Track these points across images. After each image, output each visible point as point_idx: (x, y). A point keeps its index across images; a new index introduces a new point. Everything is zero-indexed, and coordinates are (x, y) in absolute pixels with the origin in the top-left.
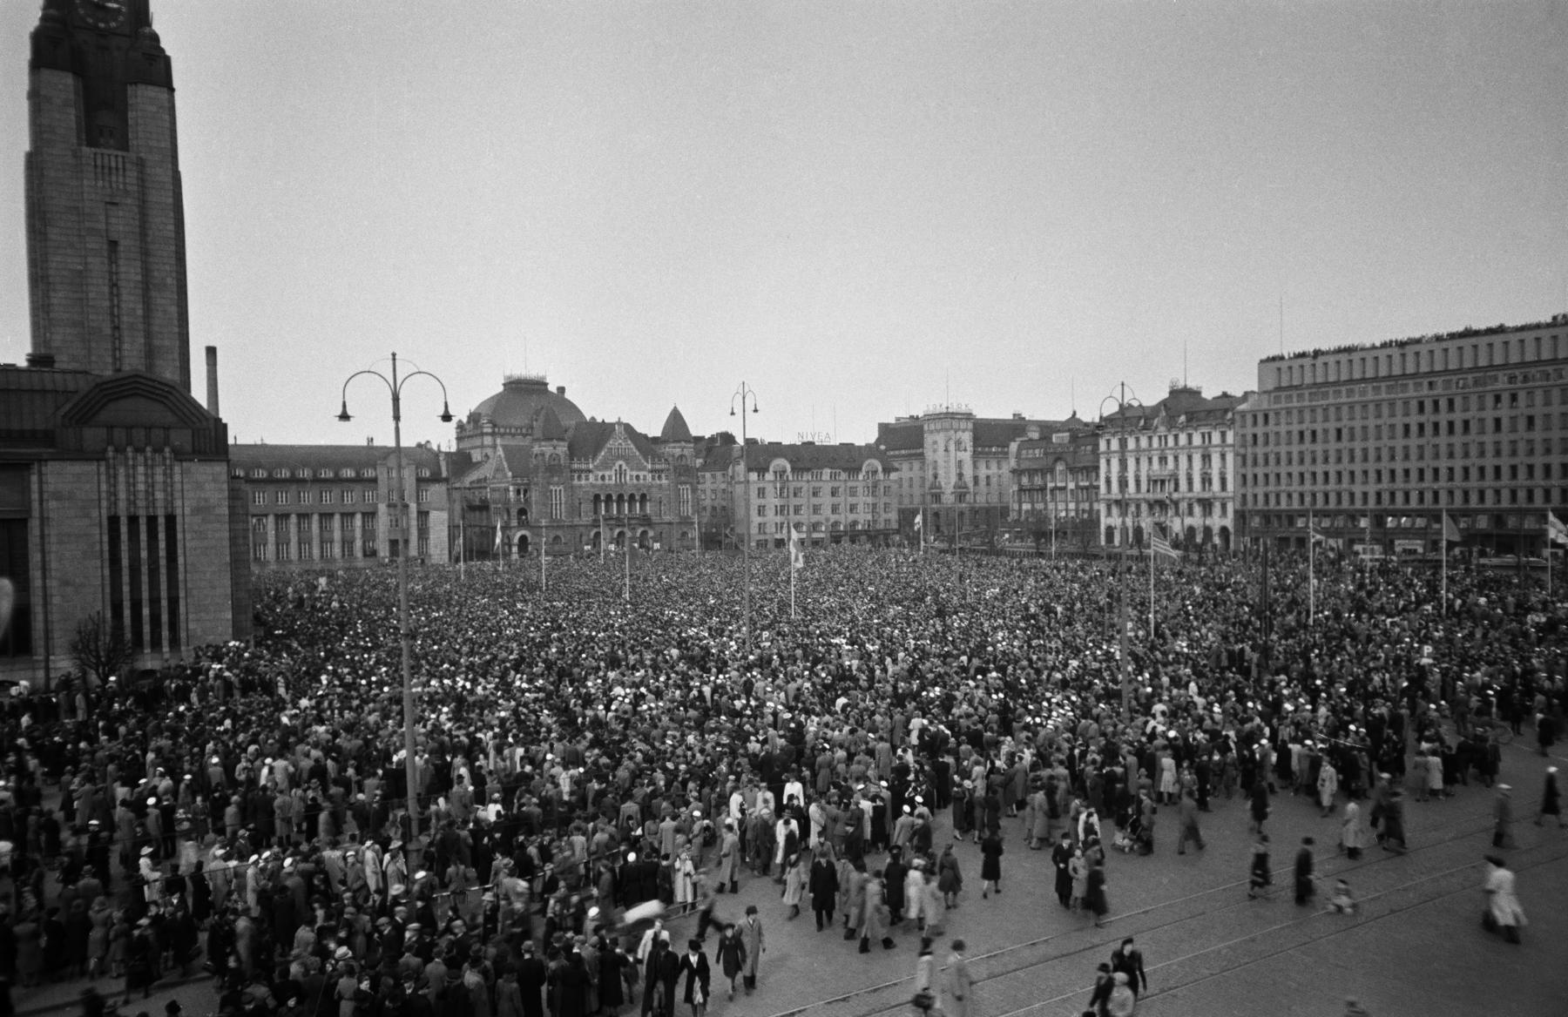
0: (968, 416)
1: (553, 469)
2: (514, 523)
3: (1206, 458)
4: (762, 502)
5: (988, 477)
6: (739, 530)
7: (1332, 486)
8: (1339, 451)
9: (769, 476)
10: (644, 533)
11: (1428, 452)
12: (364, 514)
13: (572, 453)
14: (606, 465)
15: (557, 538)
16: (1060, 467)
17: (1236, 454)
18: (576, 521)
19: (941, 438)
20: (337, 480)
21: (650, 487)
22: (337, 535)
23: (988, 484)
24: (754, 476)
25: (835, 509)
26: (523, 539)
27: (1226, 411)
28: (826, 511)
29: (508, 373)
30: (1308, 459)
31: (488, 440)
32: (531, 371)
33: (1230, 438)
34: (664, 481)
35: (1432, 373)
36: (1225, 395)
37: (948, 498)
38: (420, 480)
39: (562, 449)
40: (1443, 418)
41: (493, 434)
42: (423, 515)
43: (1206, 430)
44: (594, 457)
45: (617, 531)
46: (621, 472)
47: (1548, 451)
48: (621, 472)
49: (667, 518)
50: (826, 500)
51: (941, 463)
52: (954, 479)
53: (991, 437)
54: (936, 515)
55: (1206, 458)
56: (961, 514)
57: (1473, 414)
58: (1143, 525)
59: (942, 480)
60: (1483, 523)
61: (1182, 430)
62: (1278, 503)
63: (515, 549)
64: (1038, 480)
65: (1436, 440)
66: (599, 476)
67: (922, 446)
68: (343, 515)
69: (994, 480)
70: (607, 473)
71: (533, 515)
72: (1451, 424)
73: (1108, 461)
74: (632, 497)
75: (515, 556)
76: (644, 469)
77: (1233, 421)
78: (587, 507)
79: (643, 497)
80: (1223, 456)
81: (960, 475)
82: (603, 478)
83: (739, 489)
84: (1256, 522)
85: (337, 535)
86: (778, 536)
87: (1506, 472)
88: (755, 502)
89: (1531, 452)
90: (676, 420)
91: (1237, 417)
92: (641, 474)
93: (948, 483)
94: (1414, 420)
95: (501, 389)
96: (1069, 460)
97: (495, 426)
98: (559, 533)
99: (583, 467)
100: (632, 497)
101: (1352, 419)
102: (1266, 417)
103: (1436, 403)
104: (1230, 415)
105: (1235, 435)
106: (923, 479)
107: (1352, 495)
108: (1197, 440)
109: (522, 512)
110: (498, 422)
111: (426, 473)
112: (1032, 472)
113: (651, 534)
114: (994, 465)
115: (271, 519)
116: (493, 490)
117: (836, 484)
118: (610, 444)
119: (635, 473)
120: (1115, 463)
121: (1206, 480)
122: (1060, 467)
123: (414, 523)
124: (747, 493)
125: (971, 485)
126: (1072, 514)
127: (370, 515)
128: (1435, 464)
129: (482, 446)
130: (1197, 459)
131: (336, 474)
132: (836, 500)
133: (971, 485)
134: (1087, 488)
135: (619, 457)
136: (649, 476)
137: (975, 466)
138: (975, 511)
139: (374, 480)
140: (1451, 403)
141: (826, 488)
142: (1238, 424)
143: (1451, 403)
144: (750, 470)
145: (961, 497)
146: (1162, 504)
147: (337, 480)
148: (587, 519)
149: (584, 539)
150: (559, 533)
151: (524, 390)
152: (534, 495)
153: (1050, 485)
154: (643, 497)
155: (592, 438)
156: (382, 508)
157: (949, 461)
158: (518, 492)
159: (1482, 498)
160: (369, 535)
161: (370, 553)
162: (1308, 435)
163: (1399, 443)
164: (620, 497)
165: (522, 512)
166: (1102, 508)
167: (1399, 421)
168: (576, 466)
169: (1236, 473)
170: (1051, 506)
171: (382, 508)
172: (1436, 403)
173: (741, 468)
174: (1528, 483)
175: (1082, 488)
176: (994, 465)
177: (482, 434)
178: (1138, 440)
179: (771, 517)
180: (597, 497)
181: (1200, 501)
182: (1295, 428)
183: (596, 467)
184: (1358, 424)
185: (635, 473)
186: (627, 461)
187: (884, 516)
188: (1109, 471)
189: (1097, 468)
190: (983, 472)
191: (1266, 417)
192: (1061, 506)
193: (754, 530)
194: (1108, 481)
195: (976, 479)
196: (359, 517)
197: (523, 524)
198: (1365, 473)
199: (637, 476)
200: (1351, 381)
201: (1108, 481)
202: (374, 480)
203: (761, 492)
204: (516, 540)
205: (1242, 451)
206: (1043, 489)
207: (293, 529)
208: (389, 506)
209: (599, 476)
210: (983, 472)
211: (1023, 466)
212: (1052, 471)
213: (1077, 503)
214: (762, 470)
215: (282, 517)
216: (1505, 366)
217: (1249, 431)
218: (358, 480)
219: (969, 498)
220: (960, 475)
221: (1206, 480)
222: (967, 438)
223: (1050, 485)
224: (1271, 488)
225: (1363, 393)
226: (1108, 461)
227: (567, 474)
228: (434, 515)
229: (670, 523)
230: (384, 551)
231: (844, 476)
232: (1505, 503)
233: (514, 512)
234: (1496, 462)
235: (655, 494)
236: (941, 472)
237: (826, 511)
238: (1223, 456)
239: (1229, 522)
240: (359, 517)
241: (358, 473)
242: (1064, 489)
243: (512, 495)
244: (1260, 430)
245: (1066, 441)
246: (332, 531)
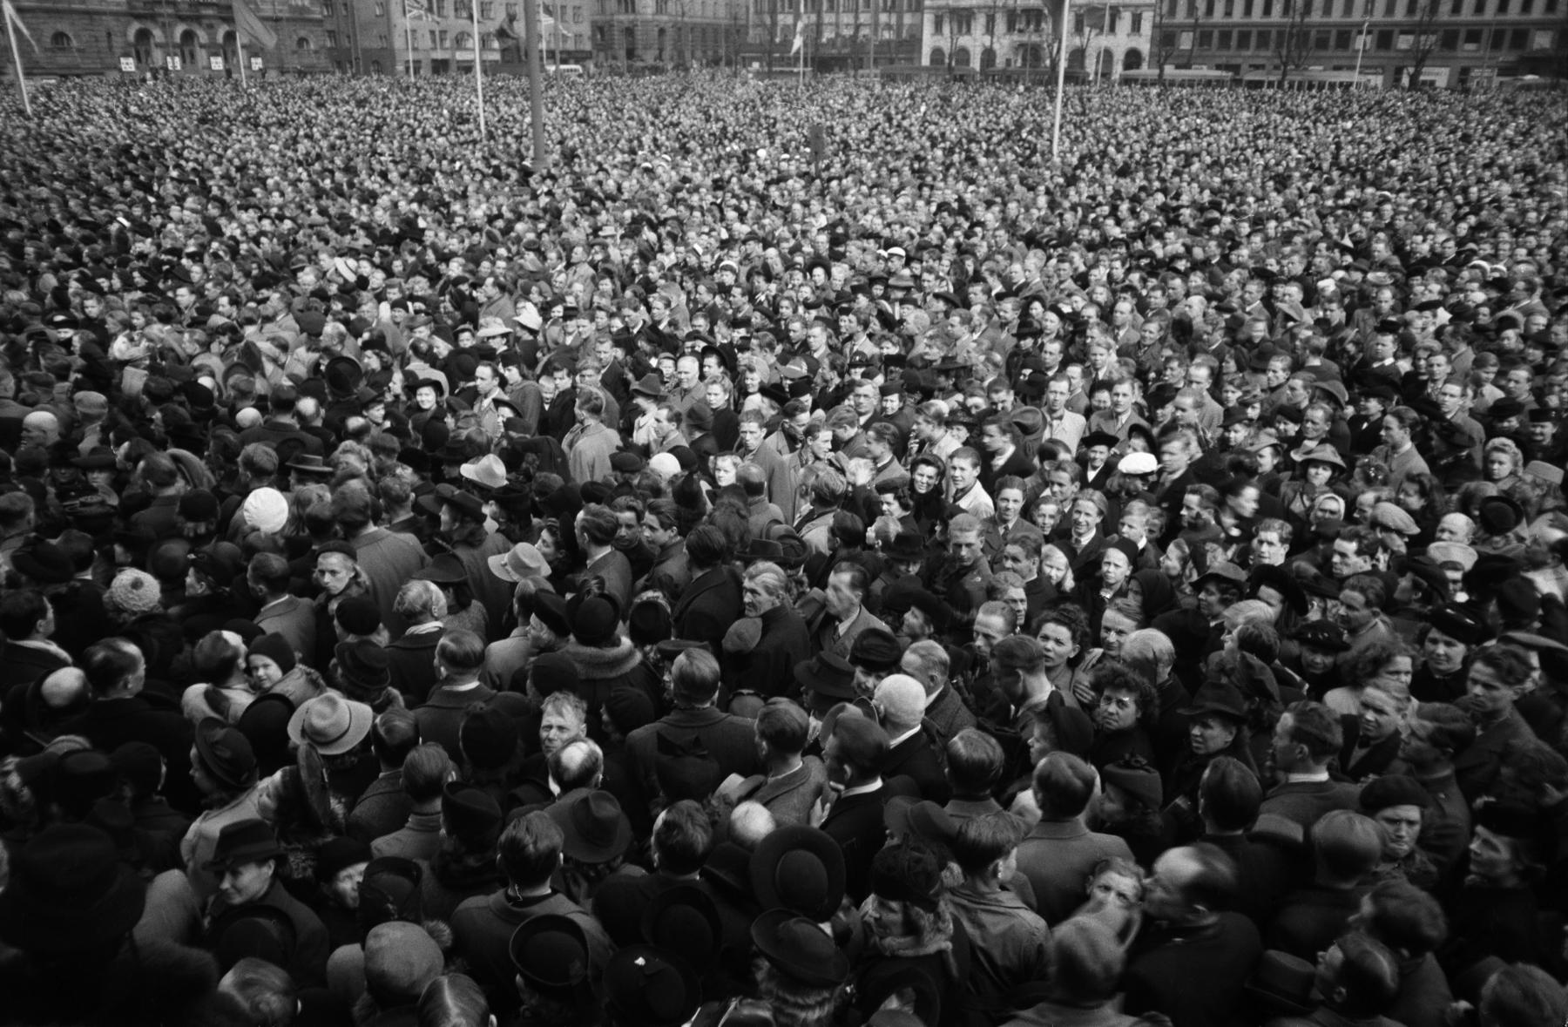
6: (369, 42)
10: (188, 36)
15: (59, 37)
45: (180, 29)
54: (629, 32)
58: (996, 46)
62: (1228, 13)
84: (1186, 42)
86: (439, 55)
126: (848, 32)
138: (679, 29)
149: (117, 42)
150: (63, 26)
170: (828, 18)
192: (847, 18)
193: (398, 43)
229: (277, 20)
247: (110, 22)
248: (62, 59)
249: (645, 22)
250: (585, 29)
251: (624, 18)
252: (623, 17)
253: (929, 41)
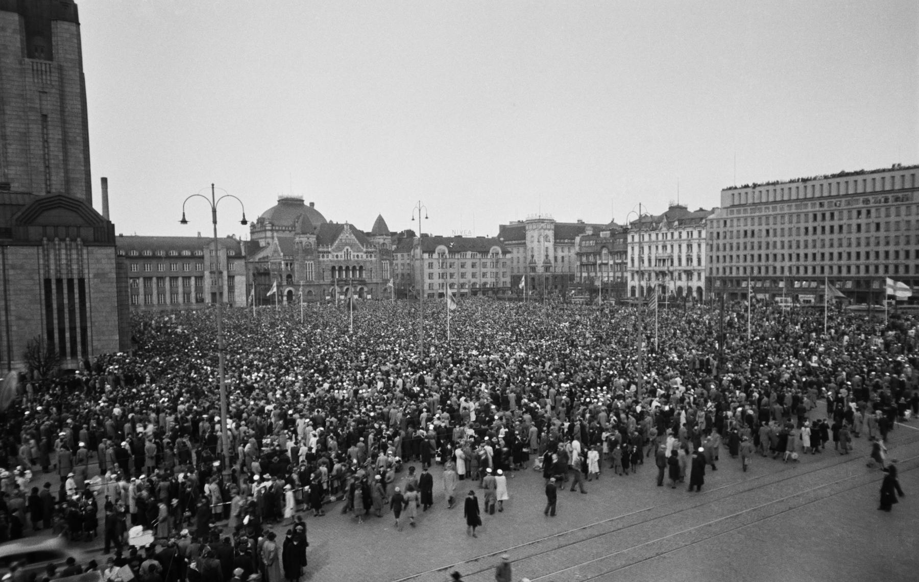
0: (552, 222)
1: (307, 251)
2: (285, 283)
3: (689, 246)
4: (431, 271)
5: (563, 257)
6: (417, 288)
7: (763, 263)
8: (745, 243)
9: (435, 256)
10: (362, 289)
11: (819, 244)
12: (196, 277)
13: (319, 242)
14: (339, 249)
15: (310, 292)
16: (605, 251)
17: (707, 244)
18: (321, 282)
19: (536, 234)
20: (180, 257)
21: (365, 262)
22: (180, 290)
23: (563, 261)
24: (426, 256)
25: (474, 275)
26: (290, 292)
27: (702, 219)
28: (469, 276)
29: (280, 194)
30: (749, 247)
31: (269, 234)
32: (294, 193)
33: (704, 235)
34: (373, 259)
35: (822, 197)
36: (701, 210)
37: (540, 270)
38: (229, 258)
39: (313, 239)
40: (827, 224)
41: (272, 230)
42: (231, 277)
43: (690, 230)
44: (331, 245)
45: (345, 288)
46: (347, 253)
47: (888, 243)
48: (347, 253)
49: (375, 280)
50: (469, 270)
51: (536, 249)
52: (543, 258)
53: (564, 233)
54: (533, 279)
55: (689, 246)
56: (547, 279)
57: (771, 226)
59: (536, 258)
60: (849, 285)
61: (676, 230)
62: (731, 273)
63: (285, 298)
64: (591, 259)
65: (753, 240)
66: (334, 255)
67: (525, 238)
68: (184, 278)
69: (566, 259)
70: (339, 254)
71: (295, 278)
72: (832, 227)
73: (633, 248)
74: (354, 268)
75: (285, 303)
76: (361, 251)
77: (706, 225)
78: (328, 274)
79: (361, 267)
80: (699, 245)
81: (547, 256)
82: (337, 256)
83: (418, 263)
84: (718, 284)
85: (180, 290)
86: (440, 291)
87: (763, 257)
88: (427, 271)
89: (850, 245)
90: (380, 222)
91: (708, 222)
92: (360, 254)
93: (540, 261)
94: (810, 225)
95: (276, 203)
96: (610, 247)
97: (273, 225)
98: (311, 289)
99: (325, 250)
100: (354, 268)
101: (753, 225)
102: (725, 222)
103: (824, 215)
104: (704, 221)
105: (707, 232)
106: (525, 258)
107: (775, 268)
108: (684, 235)
109: (289, 276)
110: (276, 223)
111: (232, 253)
112: (588, 255)
113: (366, 289)
114: (566, 250)
115: (141, 279)
116: (272, 263)
117: (474, 261)
118: (342, 236)
119: (356, 254)
120: (637, 249)
121: (689, 259)
122: (605, 251)
123: (226, 283)
124: (422, 266)
125: (553, 262)
126: (611, 279)
127: (200, 278)
128: (798, 251)
129: (266, 238)
130: (684, 247)
131: (180, 254)
132: (474, 270)
133: (553, 262)
134: (620, 264)
135: (346, 244)
136: (365, 256)
137: (555, 250)
138: (555, 277)
139: (202, 257)
140: (832, 215)
141: (469, 263)
142: (709, 226)
143: (832, 215)
144: (424, 252)
145: (547, 269)
146: (664, 274)
147: (180, 257)
148: (328, 280)
150: (311, 289)
151: (290, 204)
152: (296, 266)
153: (599, 262)
154: (361, 267)
155: (330, 233)
156: (207, 274)
157: (540, 247)
158: (287, 265)
159: (849, 271)
160: (199, 290)
161: (200, 300)
162: (749, 234)
163: (742, 241)
164: (347, 268)
165: (289, 276)
166: (629, 275)
167: (802, 225)
168: (320, 249)
169: (707, 255)
170: (599, 274)
171: (207, 274)
172: (824, 215)
173: (418, 251)
174: (876, 262)
175: (617, 264)
176: (566, 250)
177: (266, 231)
178: (650, 235)
179: (436, 281)
180: (333, 268)
181: (685, 271)
182: (742, 229)
183: (333, 250)
184: (778, 227)
185: (356, 254)
186: (351, 246)
187: (503, 280)
188: (633, 254)
189: (626, 252)
190: (560, 254)
191: (725, 222)
193: (426, 287)
194: (633, 260)
195: (556, 258)
196: (193, 279)
197: (290, 283)
198: (738, 256)
199: (359, 255)
200: (775, 202)
201: (633, 260)
202: (202, 257)
203: (431, 265)
204: (286, 293)
205: (710, 242)
206: (594, 264)
207: (154, 286)
208: (211, 273)
209: (334, 255)
210: (560, 254)
211: (584, 250)
212: (600, 254)
213: (614, 272)
214: (431, 252)
215: (148, 279)
216: (812, 199)
217: (715, 231)
218: (193, 257)
219: (552, 269)
220: (547, 256)
221: (689, 259)
222: (551, 234)
223: (599, 262)
224: (727, 264)
225: (782, 209)
226: (633, 248)
227: (316, 254)
228: (237, 279)
229: (377, 283)
230: (208, 299)
231: (479, 256)
232: (862, 274)
233: (284, 277)
234: (858, 250)
235: (368, 266)
236: (536, 254)
237: (469, 276)
238: (699, 245)
239: (702, 284)
240: (193, 279)
241: (192, 253)
242: (606, 264)
243: (283, 266)
244: (721, 230)
245: (608, 236)
246: (177, 287)
247: (325, 287)
248: (310, 298)
249: (539, 276)
250: (508, 279)
251: (532, 274)
252: (532, 274)
253: (630, 284)
